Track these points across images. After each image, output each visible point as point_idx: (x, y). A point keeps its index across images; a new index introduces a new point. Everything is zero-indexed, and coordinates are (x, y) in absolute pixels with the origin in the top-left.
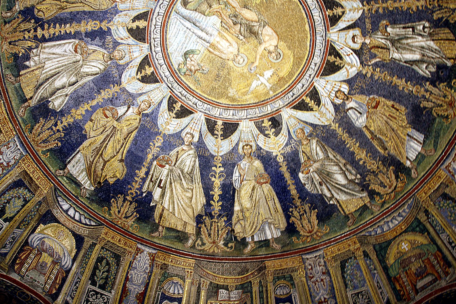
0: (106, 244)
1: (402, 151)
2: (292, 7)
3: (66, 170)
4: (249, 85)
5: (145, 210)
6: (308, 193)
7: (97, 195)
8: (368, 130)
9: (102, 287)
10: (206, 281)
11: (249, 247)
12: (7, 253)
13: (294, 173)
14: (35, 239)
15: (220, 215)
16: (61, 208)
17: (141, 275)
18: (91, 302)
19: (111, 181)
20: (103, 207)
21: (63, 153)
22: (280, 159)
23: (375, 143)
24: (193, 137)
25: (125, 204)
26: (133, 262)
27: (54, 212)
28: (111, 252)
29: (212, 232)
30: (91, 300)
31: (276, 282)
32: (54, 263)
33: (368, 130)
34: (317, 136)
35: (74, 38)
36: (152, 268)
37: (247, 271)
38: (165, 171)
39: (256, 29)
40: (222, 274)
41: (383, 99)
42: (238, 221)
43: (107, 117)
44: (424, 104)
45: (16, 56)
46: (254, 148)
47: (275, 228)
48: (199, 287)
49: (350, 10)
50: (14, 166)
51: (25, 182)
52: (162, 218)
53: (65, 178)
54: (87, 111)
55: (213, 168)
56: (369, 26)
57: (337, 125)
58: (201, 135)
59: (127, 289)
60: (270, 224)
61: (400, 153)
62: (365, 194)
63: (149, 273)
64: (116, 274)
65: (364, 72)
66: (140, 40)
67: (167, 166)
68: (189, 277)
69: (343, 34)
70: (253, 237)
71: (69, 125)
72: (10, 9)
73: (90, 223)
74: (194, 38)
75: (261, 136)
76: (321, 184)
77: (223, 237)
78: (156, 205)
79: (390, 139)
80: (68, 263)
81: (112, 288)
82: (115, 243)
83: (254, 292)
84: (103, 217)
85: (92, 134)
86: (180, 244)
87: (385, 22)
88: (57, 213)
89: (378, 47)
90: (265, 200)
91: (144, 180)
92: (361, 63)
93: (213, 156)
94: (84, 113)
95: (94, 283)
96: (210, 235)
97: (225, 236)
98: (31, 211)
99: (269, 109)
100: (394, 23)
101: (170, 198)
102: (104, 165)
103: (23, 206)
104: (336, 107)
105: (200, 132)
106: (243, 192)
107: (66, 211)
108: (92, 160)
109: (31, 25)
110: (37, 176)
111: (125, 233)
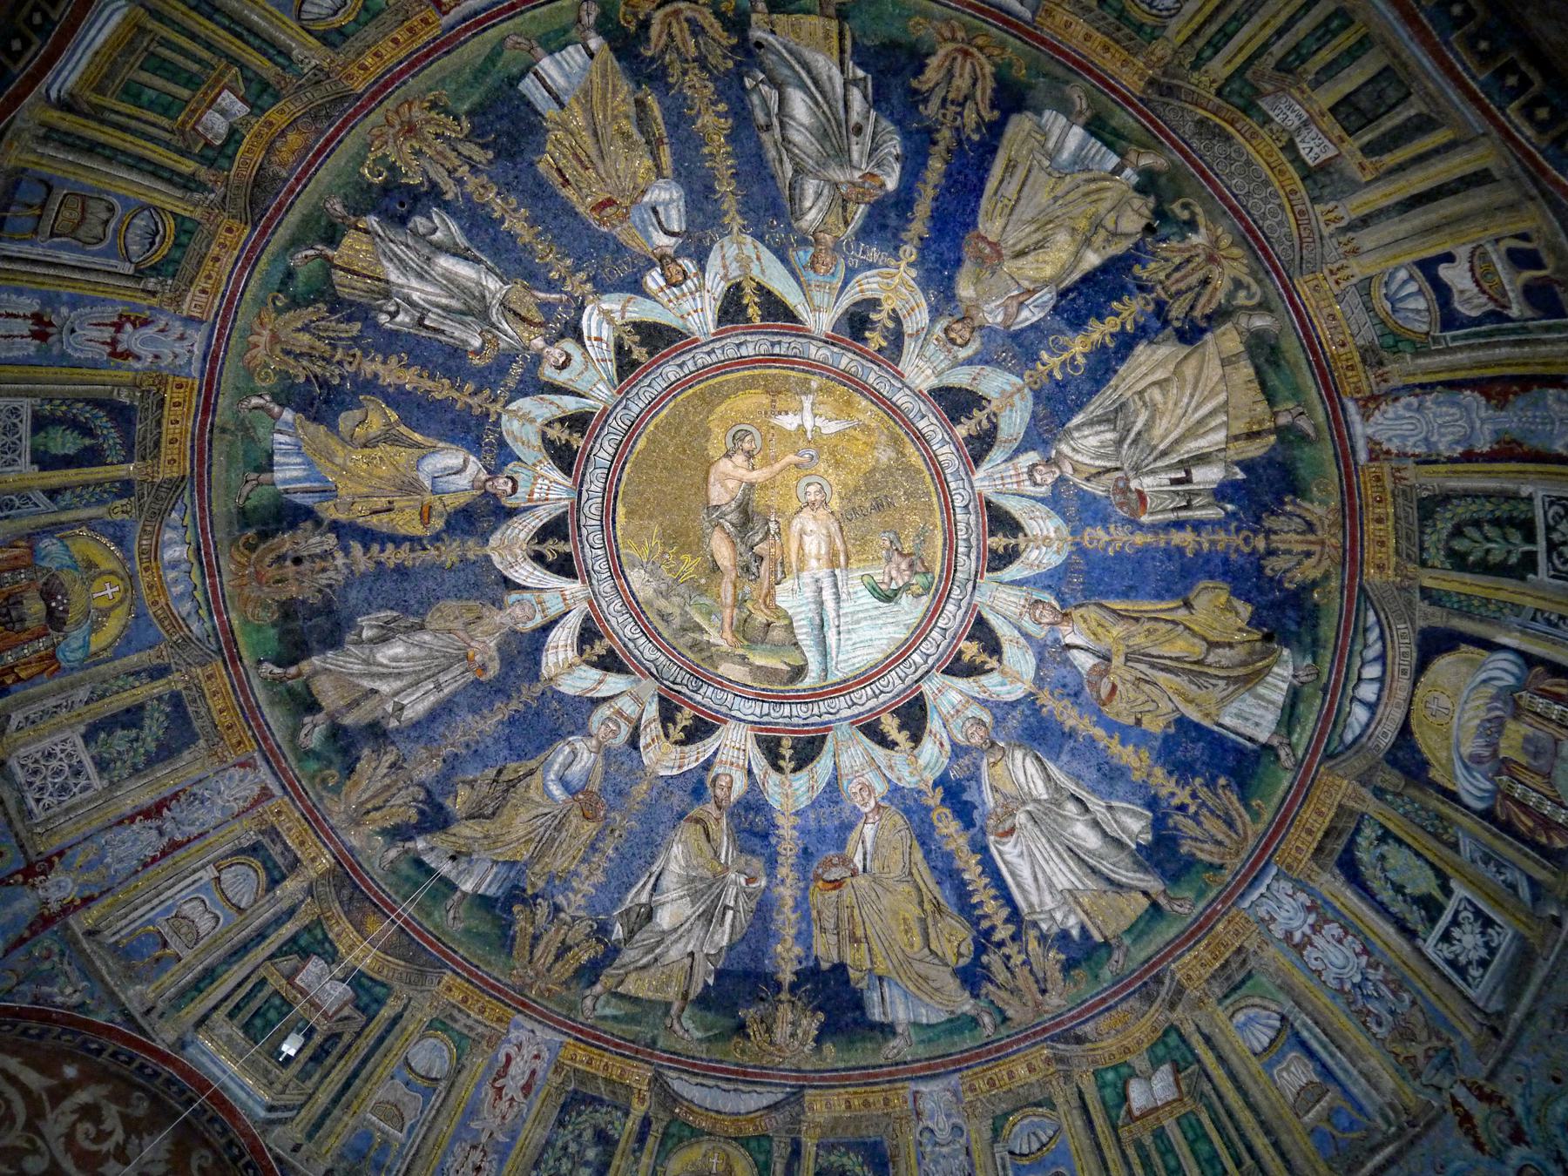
1: (597, 80)
2: (635, 499)
3: (1275, 742)
4: (840, 434)
5: (1265, 486)
6: (907, 135)
7: (1298, 635)
8: (657, 166)
10: (1322, 219)
11: (1146, 161)
12: (1529, 878)
13: (903, 201)
14: (1473, 787)
15: (1142, 288)
16: (1368, 725)
19: (1245, 610)
20: (1316, 605)
21: (1239, 764)
22: (909, 252)
23: (660, 129)
24: (1033, 467)
25: (1283, 547)
27: (1386, 742)
28: (1422, 533)
29: (1193, 280)
31: (1154, 28)
32: (1517, 712)
33: (657, 166)
34: (789, 228)
35: (985, 849)
37: (1202, 122)
38: (1148, 483)
39: (733, 517)
40: (1267, 183)
41: (580, 209)
42: (1114, 234)
43: (1114, 687)
44: (480, 156)
45: (1068, 967)
46: (943, 323)
47: (1046, 135)
49: (533, 421)
50: (1310, 892)
51: (1340, 848)
53: (1295, 738)
54: (1123, 743)
55: (1059, 377)
56: (516, 370)
57: (726, 220)
58: (1018, 452)
60: (1051, 158)
61: (604, 76)
62: (757, 34)
65: (589, 286)
66: (923, 708)
67: (1134, 484)
68: (1347, 272)
69: (580, 386)
70: (1117, 171)
71: (1170, 773)
72: (974, 1022)
74: (847, 607)
75: (909, 327)
76: (859, 130)
78: (1238, 463)
79: (615, 118)
83: (1230, 69)
85: (1166, 707)
87: (476, 361)
88: (1386, 735)
89: (524, 319)
90: (1019, 209)
91: (1198, 526)
92: (581, 308)
93: (1037, 395)
94: (1131, 748)
95: (1529, 562)
96: (1205, 282)
97: (1174, 243)
98: (1405, 815)
99: (846, 361)
100: (457, 352)
101: (1197, 437)
102: (1218, 645)
103: (1400, 841)
104: (701, 258)
105: (1010, 459)
106: (1049, 271)
107: (1372, 707)
108: (1222, 683)
109: (992, 959)
110: (1315, 819)
111: (1351, 512)
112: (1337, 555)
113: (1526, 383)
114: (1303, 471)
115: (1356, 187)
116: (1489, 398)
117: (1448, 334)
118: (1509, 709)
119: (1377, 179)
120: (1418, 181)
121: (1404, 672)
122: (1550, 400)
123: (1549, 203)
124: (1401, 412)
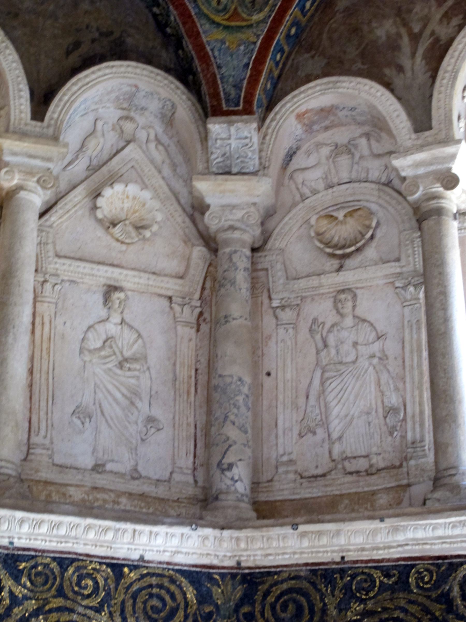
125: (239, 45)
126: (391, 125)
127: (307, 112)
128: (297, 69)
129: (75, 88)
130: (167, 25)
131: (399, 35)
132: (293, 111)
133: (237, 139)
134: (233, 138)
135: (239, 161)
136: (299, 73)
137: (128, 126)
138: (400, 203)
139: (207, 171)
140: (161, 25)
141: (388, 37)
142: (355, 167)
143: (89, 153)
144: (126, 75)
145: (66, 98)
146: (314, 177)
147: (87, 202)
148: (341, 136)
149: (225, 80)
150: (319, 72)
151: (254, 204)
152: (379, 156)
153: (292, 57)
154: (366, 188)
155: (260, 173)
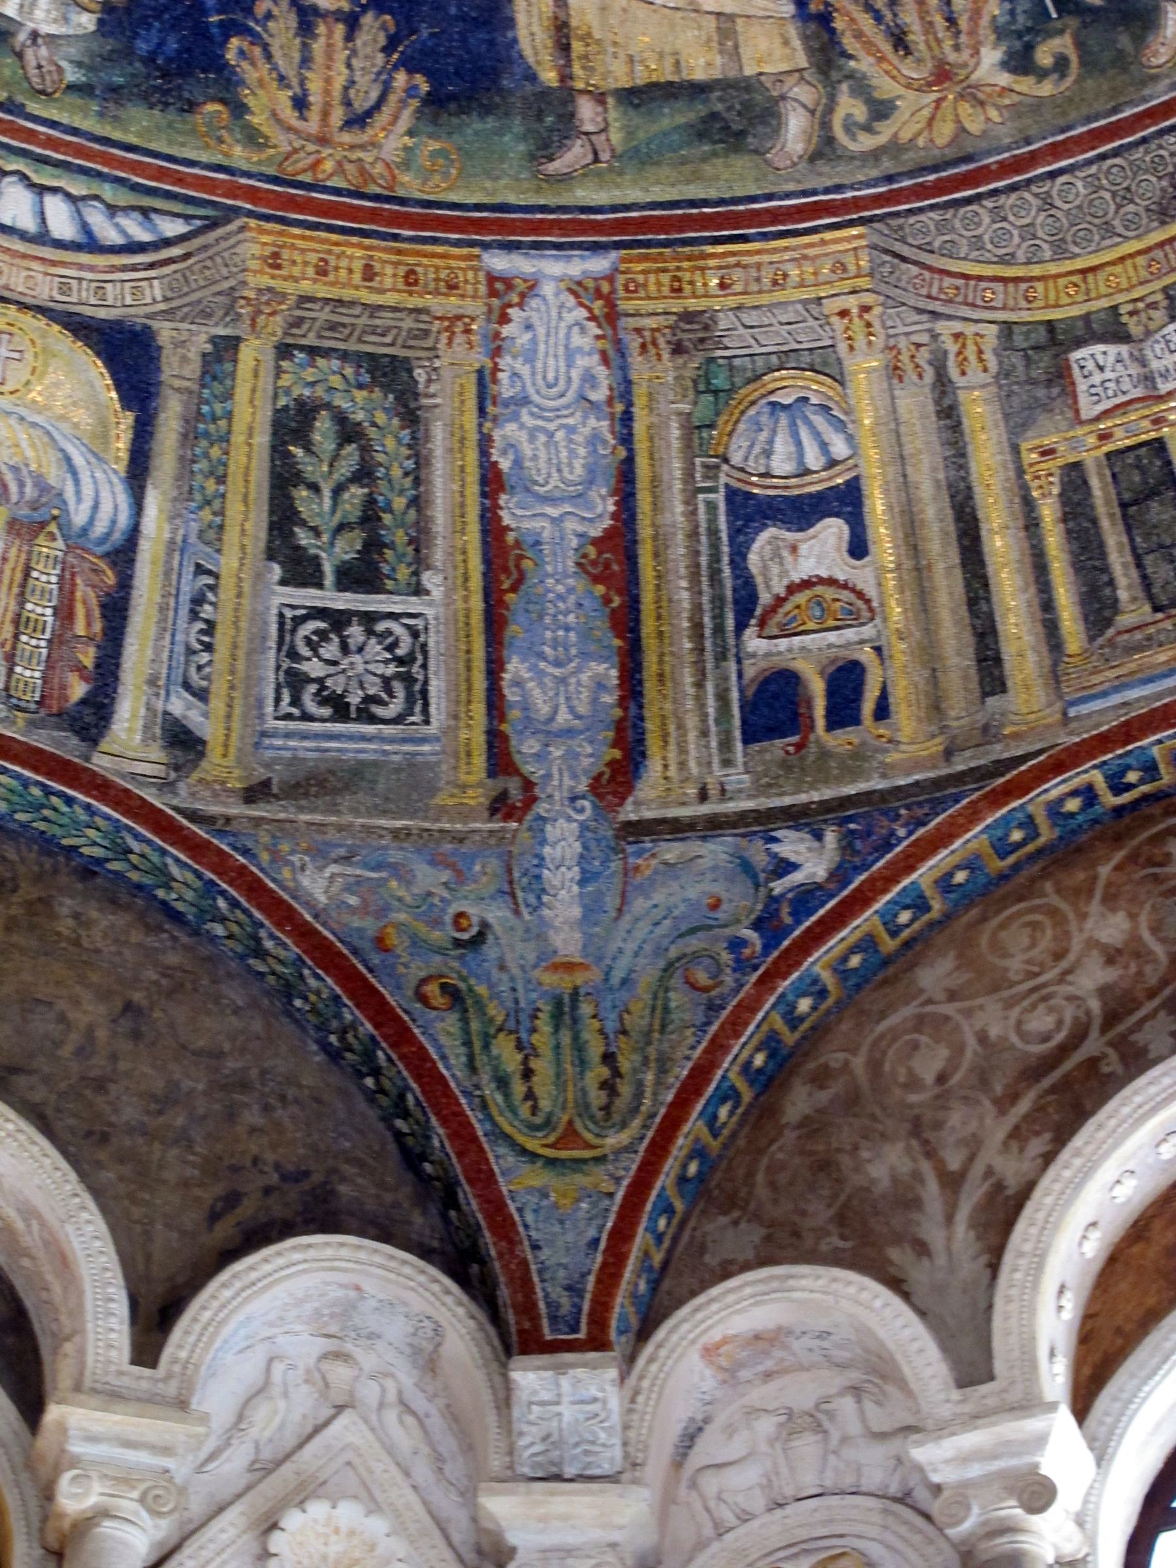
0: (298, 322)
7: (128, 53)
9: (362, 575)
10: (969, 329)
17: (571, 430)
18: (320, 681)
20: (191, 107)
25: (318, 47)
26: (496, 369)
28: (344, 356)
30: (314, 668)
36: (624, 368)
40: (1060, 251)
48: (942, 383)
52: (577, 47)
59: (511, 537)
63: (610, 401)
64: (418, 475)
68: (860, 341)
73: (153, 229)
77: (985, 21)
80: (106, 509)
81: (420, 562)
82: (348, 294)
84: (219, 168)
86: (741, 163)
95: (301, 570)
96: (900, 41)
112: (298, 167)
113: (626, 622)
114: (477, 124)
115: (1017, 423)
116: (595, 542)
117: (720, 498)
118: (24, 511)
119: (1020, 472)
120: (1001, 544)
121: (65, 289)
122: (601, 668)
123: (938, 784)
124: (582, 362)
125: (578, 1200)
126: (907, 1371)
127: (725, 1341)
128: (703, 1249)
129: (227, 1293)
130: (423, 1157)
131: (917, 1176)
132: (693, 1342)
133: (574, 1403)
134: (566, 1399)
135: (578, 1450)
136: (707, 1258)
137: (340, 1373)
138: (931, 1542)
139: (509, 1473)
140: (412, 1157)
141: (895, 1180)
142: (832, 1459)
143: (254, 1433)
144: (336, 1264)
145: (207, 1315)
146: (743, 1483)
147: (249, 1543)
148: (802, 1392)
149: (547, 1276)
150: (750, 1254)
151: (613, 1545)
152: (882, 1436)
153: (692, 1223)
154: (856, 1507)
155: (625, 1477)
